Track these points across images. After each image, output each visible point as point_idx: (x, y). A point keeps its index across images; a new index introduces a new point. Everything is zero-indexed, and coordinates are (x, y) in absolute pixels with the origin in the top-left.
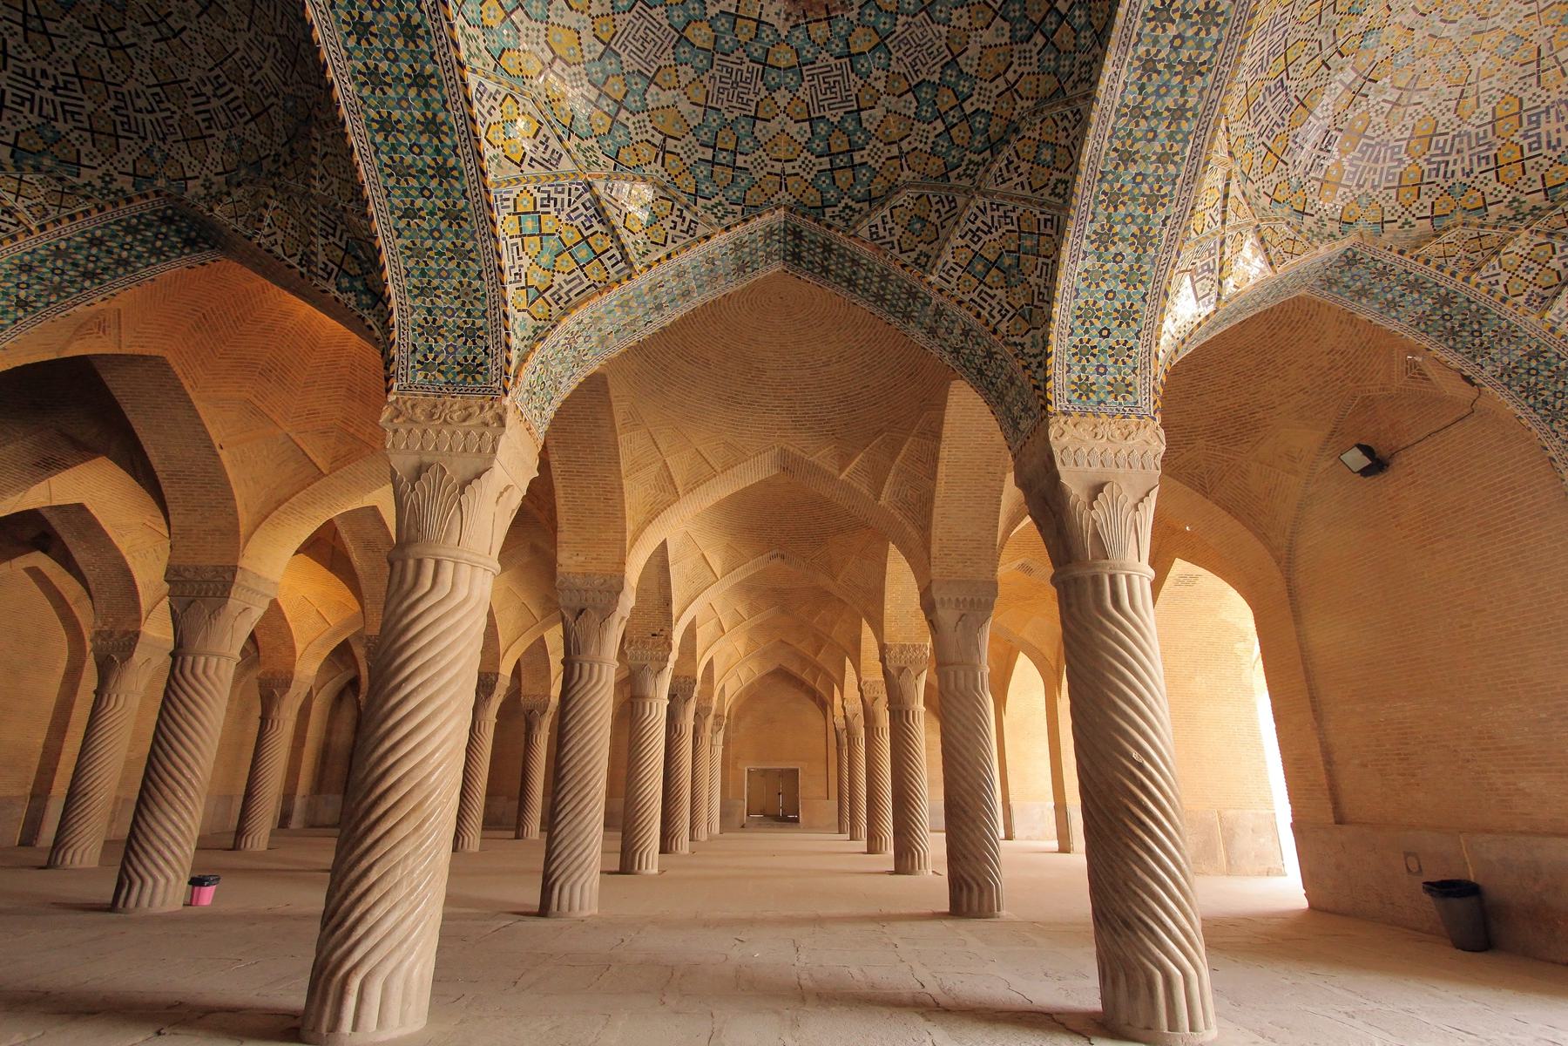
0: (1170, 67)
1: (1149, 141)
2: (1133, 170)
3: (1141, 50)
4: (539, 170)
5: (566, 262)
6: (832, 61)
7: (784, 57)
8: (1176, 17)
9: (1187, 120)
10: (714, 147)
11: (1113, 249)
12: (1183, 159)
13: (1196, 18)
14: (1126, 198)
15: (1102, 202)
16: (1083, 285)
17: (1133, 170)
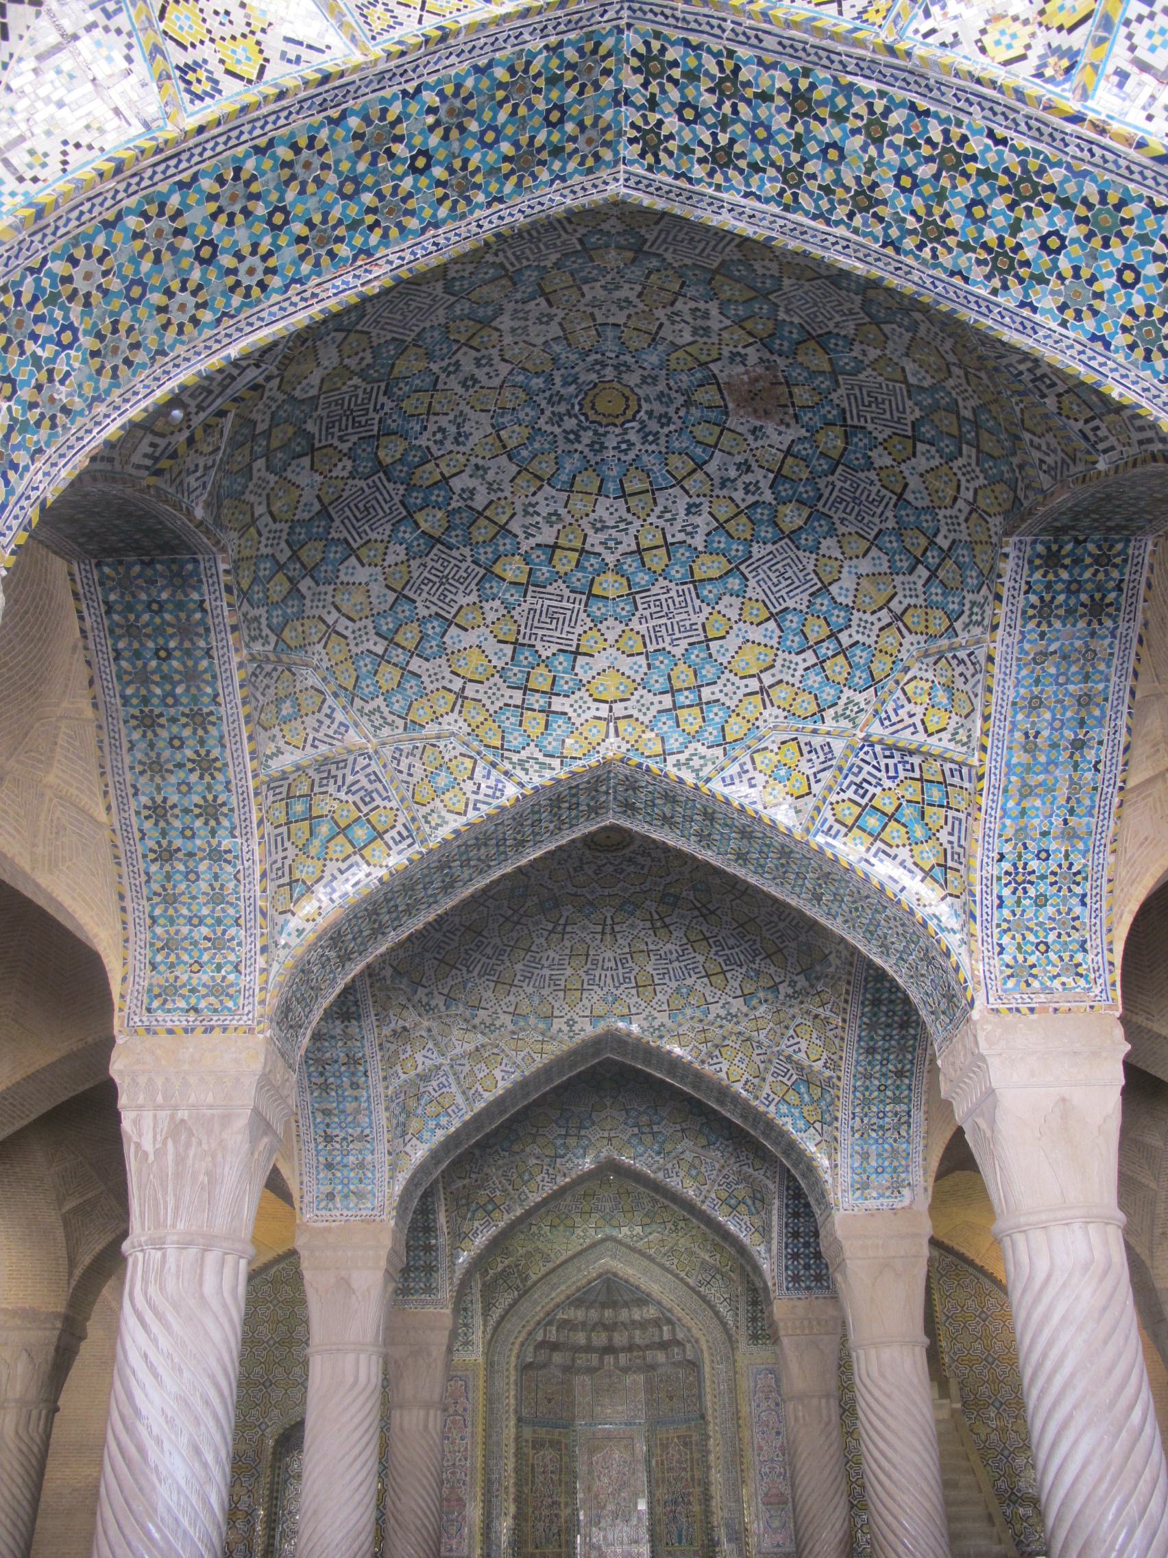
0: (724, 124)
1: (842, 157)
2: (887, 189)
3: (698, 171)
4: (826, 776)
5: (935, 816)
6: (842, 391)
7: (832, 440)
8: (653, 117)
9: (813, 87)
10: (918, 562)
11: (1029, 253)
12: (882, 94)
13: (654, 88)
14: (937, 212)
15: (935, 256)
16: (1089, 324)
17: (887, 189)
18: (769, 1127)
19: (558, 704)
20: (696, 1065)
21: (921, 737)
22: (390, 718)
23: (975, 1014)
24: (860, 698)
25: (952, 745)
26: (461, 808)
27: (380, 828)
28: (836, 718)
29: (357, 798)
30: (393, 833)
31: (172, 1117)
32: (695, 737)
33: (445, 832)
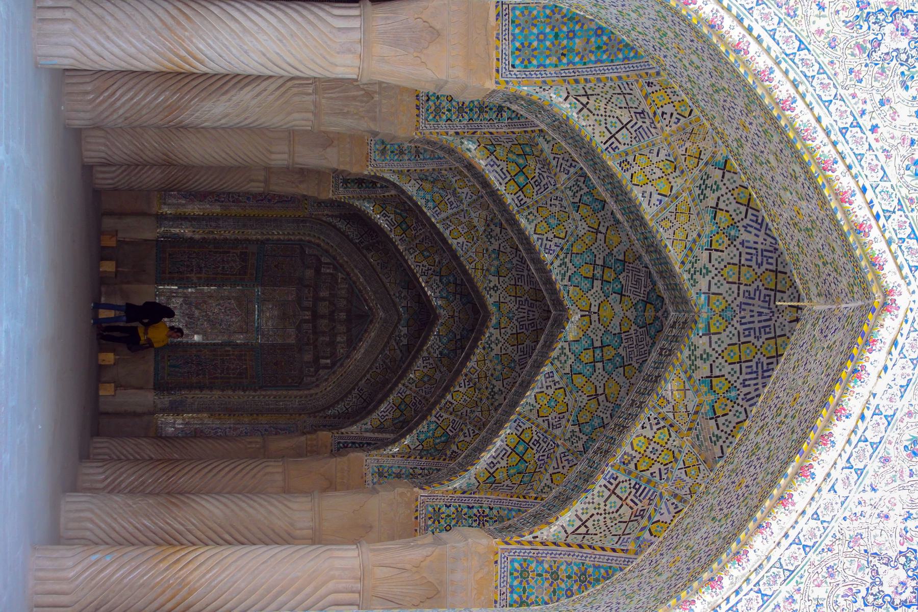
4: (545, 425)
5: (517, 479)
18: (424, 417)
19: (597, 283)
20: (464, 371)
21: (551, 471)
22: (578, 195)
23: (416, 489)
24: (580, 444)
25: (543, 484)
26: (539, 231)
27: (524, 189)
28: (573, 431)
29: (537, 178)
30: (522, 196)
31: (375, 92)
32: (578, 358)
33: (523, 222)
